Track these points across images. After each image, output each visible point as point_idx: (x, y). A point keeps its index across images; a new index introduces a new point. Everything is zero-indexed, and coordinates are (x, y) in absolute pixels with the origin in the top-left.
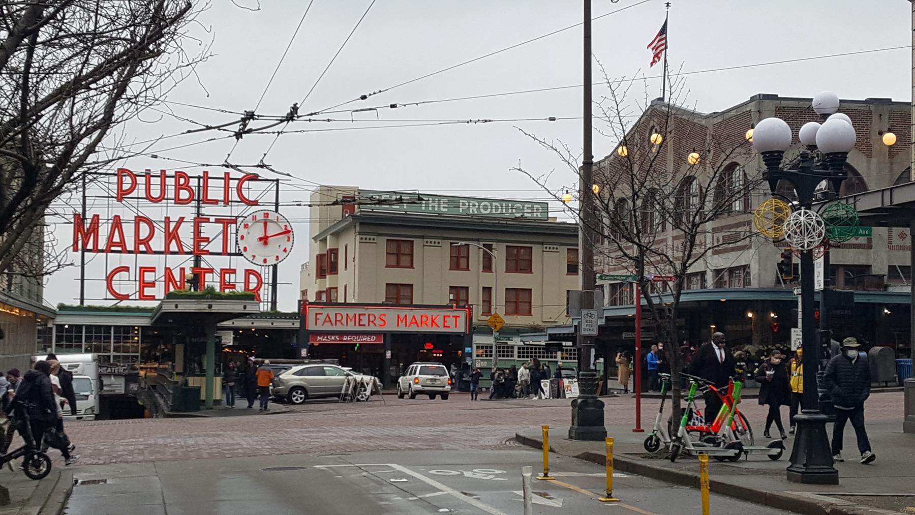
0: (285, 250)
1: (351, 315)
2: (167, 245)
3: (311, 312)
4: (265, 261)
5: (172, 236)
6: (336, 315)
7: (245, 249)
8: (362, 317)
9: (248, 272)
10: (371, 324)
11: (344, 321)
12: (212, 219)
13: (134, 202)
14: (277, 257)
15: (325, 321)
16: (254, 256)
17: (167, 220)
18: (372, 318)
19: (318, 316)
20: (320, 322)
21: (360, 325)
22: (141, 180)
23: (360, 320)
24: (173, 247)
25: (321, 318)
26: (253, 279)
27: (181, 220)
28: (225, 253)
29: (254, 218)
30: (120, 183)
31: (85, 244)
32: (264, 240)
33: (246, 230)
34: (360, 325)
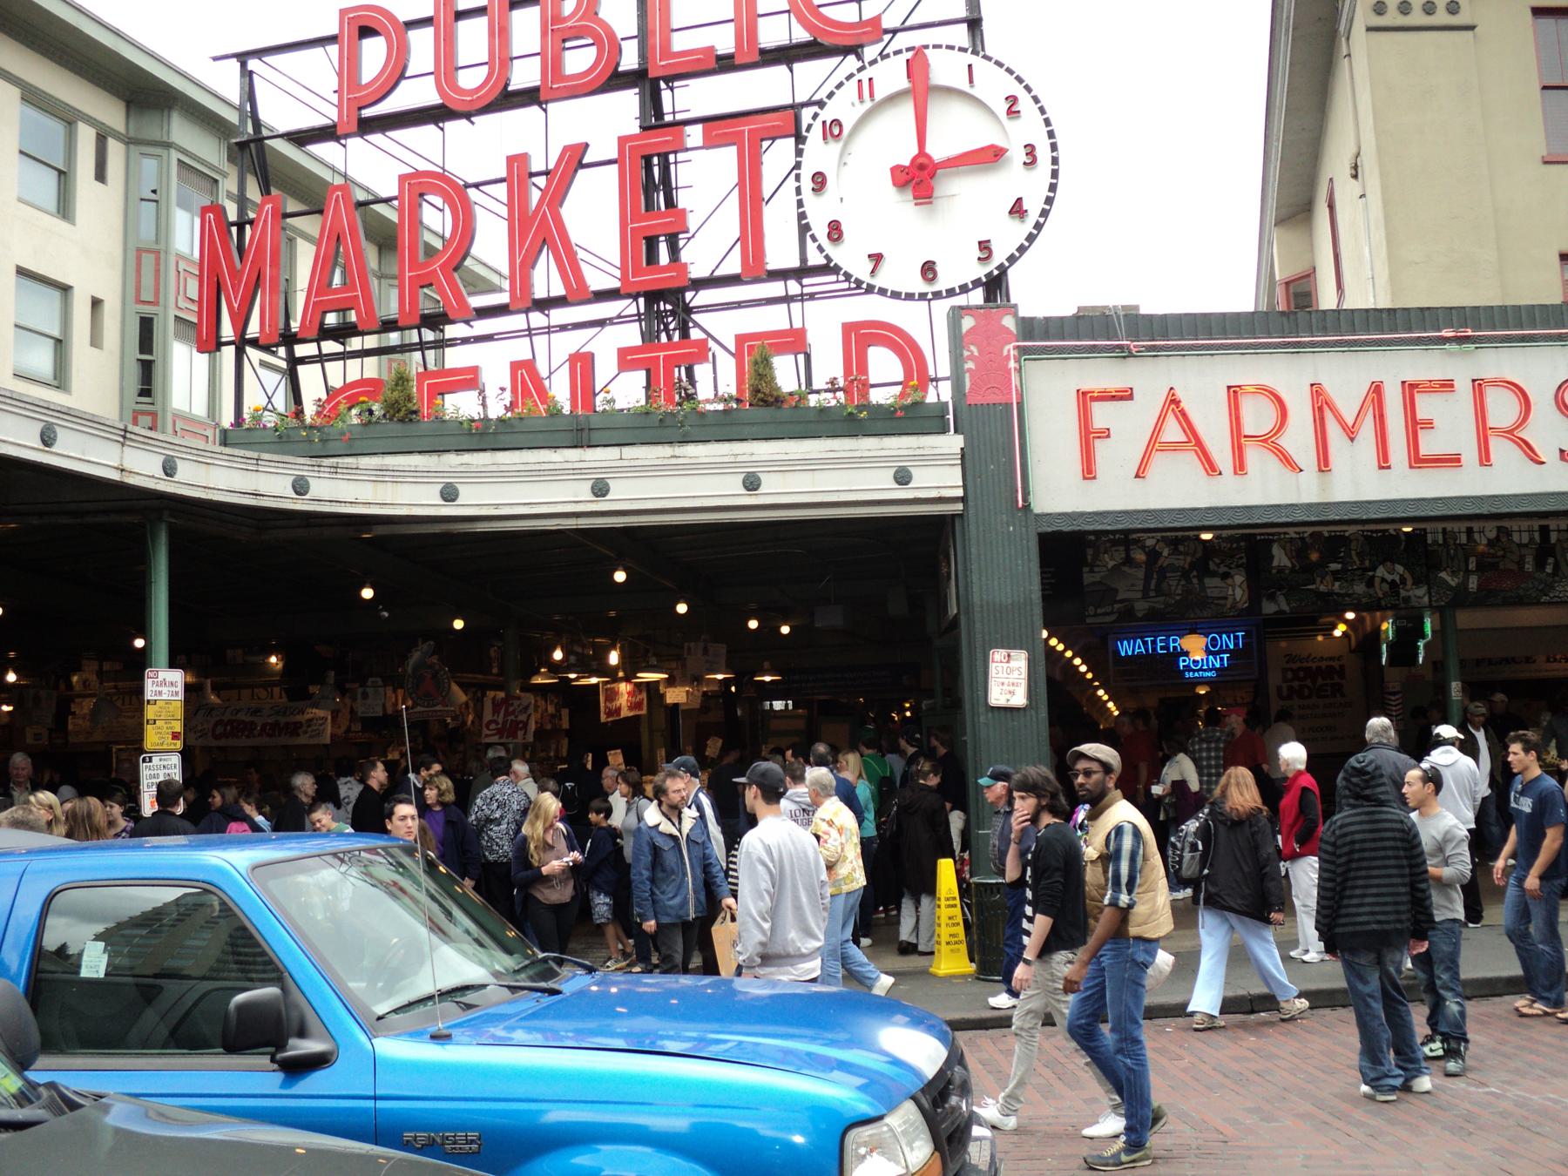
0: (1018, 210)
1: (1348, 399)
2: (522, 268)
3: (1049, 393)
4: (929, 270)
5: (538, 230)
6: (1234, 393)
7: (835, 231)
8: (1426, 406)
9: (859, 337)
10: (1498, 446)
11: (1299, 438)
12: (695, 134)
13: (423, 137)
14: (984, 246)
15: (1154, 444)
16: (877, 258)
17: (518, 162)
18: (1502, 409)
19: (1102, 414)
20: (1117, 456)
21: (1417, 460)
22: (422, 44)
23: (1415, 426)
24: (546, 279)
25: (1127, 427)
26: (884, 365)
27: (575, 159)
28: (754, 270)
29: (866, 89)
30: (349, 67)
31: (241, 323)
32: (918, 179)
33: (835, 147)
34: (1417, 460)
